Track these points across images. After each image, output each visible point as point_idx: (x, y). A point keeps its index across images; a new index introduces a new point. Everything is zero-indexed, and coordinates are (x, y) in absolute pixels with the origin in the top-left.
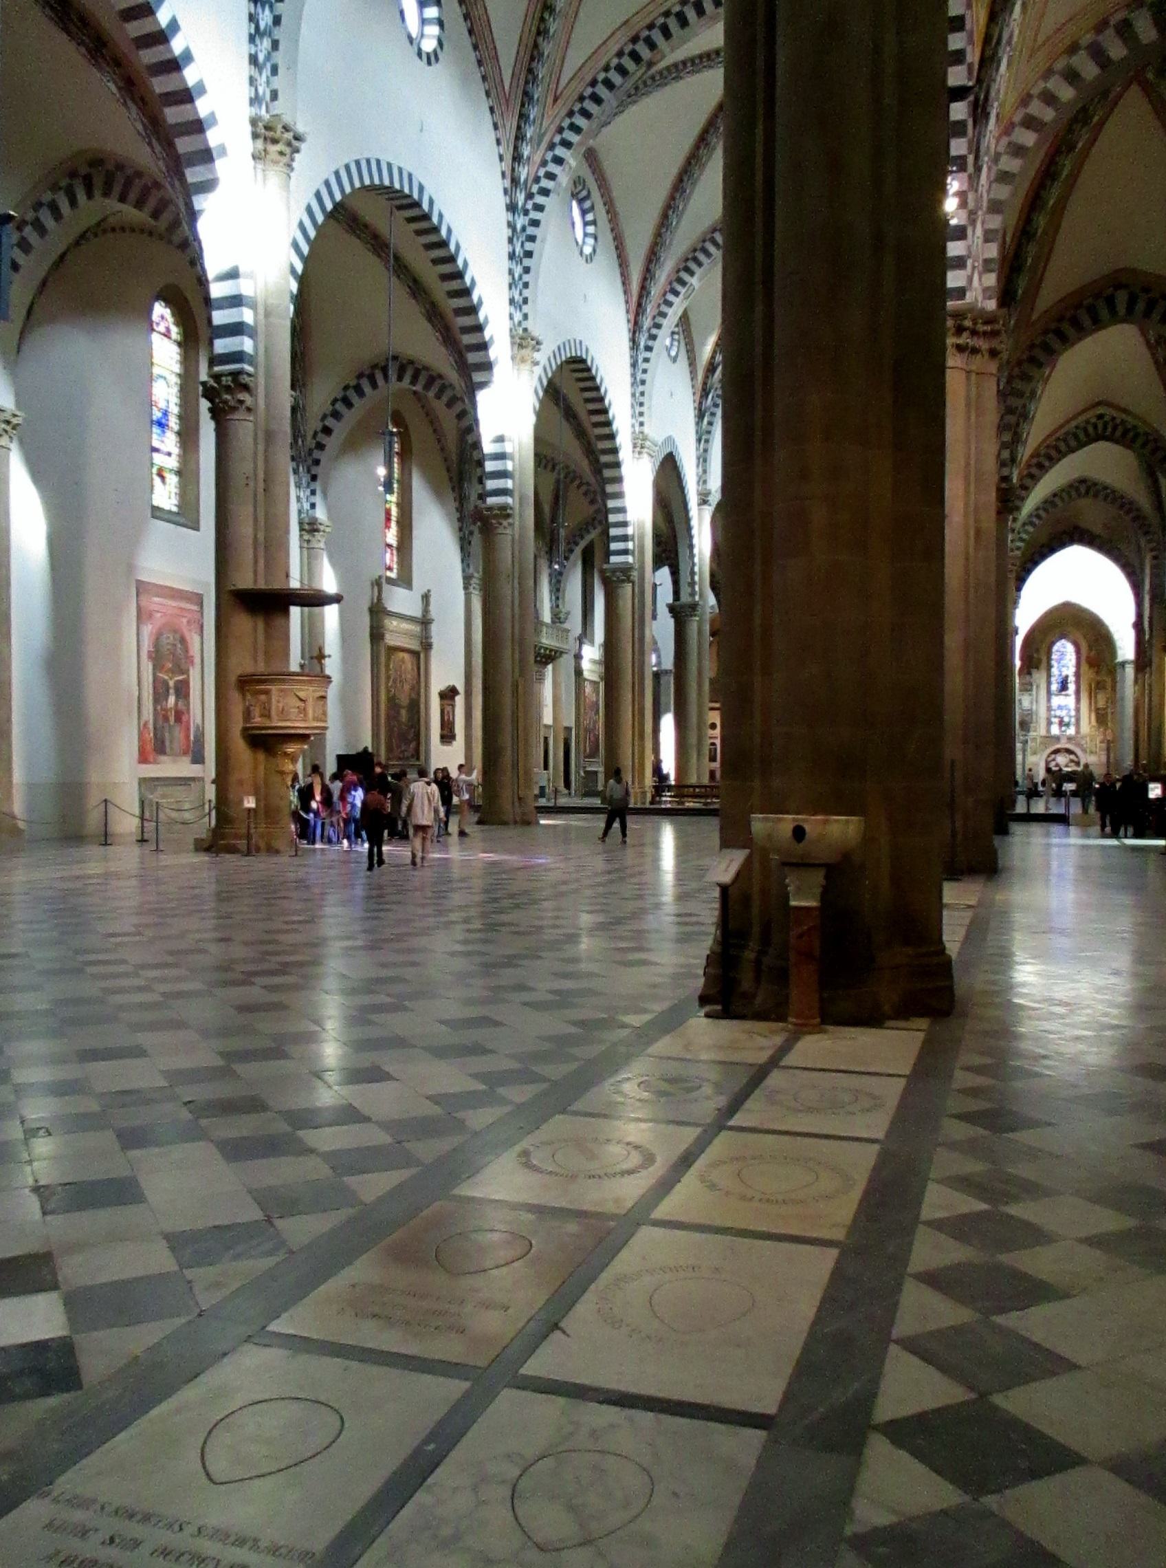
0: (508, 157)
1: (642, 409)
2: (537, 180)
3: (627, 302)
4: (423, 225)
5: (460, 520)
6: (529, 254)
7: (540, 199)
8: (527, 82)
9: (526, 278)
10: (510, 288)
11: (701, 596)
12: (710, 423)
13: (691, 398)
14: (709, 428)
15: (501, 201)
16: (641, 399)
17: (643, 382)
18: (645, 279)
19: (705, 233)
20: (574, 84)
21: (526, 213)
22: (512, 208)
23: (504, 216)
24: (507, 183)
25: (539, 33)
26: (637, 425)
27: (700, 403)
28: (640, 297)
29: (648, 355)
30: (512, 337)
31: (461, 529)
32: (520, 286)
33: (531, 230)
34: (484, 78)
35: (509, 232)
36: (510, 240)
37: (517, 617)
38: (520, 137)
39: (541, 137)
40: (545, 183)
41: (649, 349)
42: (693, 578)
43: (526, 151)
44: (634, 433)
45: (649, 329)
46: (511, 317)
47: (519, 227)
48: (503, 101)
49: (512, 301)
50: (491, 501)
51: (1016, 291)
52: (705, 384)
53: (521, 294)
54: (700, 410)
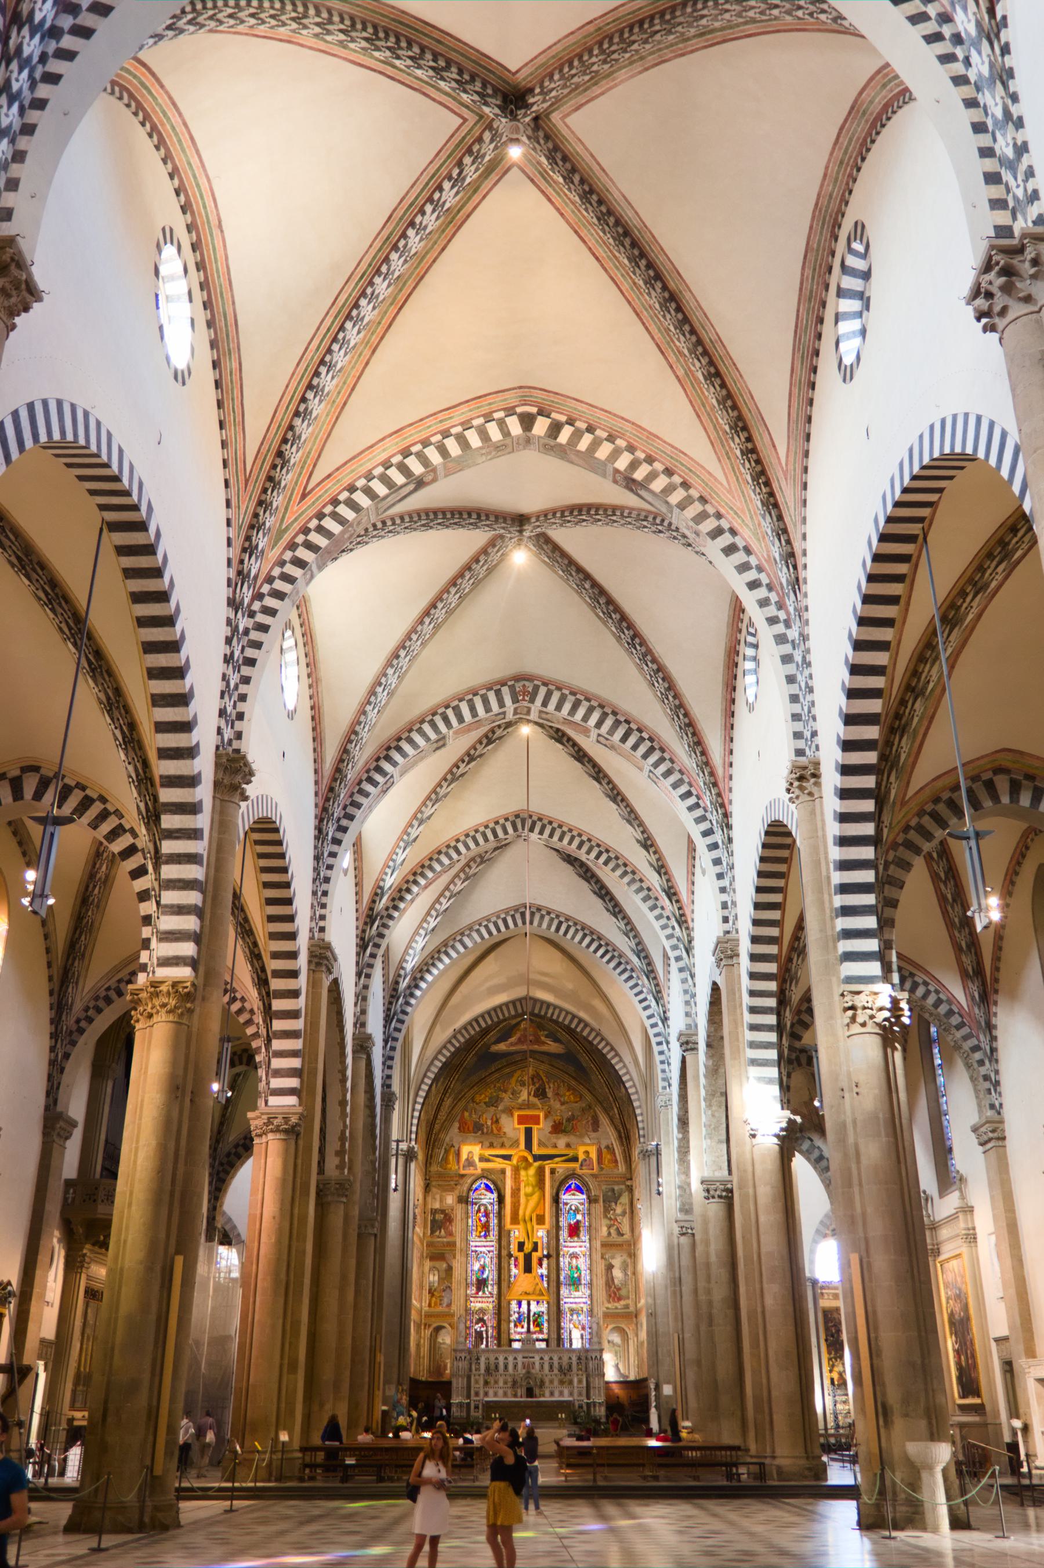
0: (238, 544)
1: (323, 912)
2: (270, 580)
3: (316, 783)
4: (142, 562)
5: (54, 1036)
6: (251, 662)
7: (270, 602)
8: (274, 467)
9: (243, 689)
10: (222, 697)
11: (350, 1169)
12: (373, 956)
13: (354, 923)
14: (371, 961)
15: (223, 593)
16: (324, 900)
17: (327, 880)
18: (341, 761)
19: (413, 723)
20: (328, 484)
21: (252, 614)
22: (233, 603)
23: (224, 611)
24: (232, 574)
25: (297, 414)
26: (316, 930)
27: (364, 931)
28: (335, 780)
29: (335, 848)
30: (218, 756)
31: (52, 1049)
32: (235, 697)
33: (254, 635)
34: (224, 444)
35: (227, 631)
36: (228, 641)
37: (182, 1153)
38: (255, 525)
39: (281, 533)
40: (279, 585)
41: (337, 842)
42: (343, 1145)
43: (262, 541)
44: (312, 938)
45: (339, 819)
46: (219, 731)
47: (241, 629)
48: (242, 478)
49: (222, 713)
50: (162, 973)
51: (898, 756)
52: (371, 909)
53: (234, 707)
54: (362, 939)
